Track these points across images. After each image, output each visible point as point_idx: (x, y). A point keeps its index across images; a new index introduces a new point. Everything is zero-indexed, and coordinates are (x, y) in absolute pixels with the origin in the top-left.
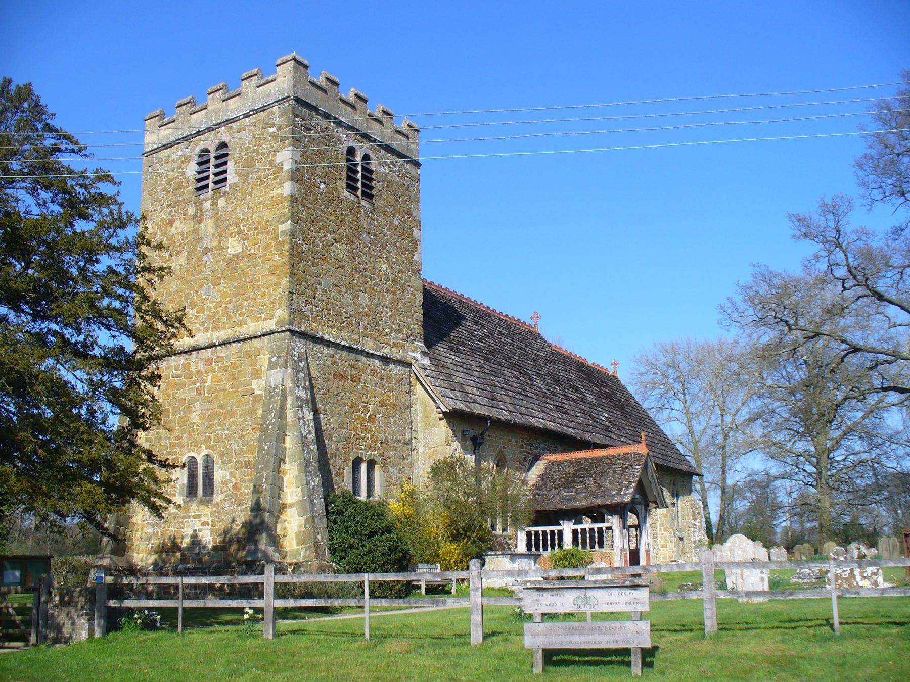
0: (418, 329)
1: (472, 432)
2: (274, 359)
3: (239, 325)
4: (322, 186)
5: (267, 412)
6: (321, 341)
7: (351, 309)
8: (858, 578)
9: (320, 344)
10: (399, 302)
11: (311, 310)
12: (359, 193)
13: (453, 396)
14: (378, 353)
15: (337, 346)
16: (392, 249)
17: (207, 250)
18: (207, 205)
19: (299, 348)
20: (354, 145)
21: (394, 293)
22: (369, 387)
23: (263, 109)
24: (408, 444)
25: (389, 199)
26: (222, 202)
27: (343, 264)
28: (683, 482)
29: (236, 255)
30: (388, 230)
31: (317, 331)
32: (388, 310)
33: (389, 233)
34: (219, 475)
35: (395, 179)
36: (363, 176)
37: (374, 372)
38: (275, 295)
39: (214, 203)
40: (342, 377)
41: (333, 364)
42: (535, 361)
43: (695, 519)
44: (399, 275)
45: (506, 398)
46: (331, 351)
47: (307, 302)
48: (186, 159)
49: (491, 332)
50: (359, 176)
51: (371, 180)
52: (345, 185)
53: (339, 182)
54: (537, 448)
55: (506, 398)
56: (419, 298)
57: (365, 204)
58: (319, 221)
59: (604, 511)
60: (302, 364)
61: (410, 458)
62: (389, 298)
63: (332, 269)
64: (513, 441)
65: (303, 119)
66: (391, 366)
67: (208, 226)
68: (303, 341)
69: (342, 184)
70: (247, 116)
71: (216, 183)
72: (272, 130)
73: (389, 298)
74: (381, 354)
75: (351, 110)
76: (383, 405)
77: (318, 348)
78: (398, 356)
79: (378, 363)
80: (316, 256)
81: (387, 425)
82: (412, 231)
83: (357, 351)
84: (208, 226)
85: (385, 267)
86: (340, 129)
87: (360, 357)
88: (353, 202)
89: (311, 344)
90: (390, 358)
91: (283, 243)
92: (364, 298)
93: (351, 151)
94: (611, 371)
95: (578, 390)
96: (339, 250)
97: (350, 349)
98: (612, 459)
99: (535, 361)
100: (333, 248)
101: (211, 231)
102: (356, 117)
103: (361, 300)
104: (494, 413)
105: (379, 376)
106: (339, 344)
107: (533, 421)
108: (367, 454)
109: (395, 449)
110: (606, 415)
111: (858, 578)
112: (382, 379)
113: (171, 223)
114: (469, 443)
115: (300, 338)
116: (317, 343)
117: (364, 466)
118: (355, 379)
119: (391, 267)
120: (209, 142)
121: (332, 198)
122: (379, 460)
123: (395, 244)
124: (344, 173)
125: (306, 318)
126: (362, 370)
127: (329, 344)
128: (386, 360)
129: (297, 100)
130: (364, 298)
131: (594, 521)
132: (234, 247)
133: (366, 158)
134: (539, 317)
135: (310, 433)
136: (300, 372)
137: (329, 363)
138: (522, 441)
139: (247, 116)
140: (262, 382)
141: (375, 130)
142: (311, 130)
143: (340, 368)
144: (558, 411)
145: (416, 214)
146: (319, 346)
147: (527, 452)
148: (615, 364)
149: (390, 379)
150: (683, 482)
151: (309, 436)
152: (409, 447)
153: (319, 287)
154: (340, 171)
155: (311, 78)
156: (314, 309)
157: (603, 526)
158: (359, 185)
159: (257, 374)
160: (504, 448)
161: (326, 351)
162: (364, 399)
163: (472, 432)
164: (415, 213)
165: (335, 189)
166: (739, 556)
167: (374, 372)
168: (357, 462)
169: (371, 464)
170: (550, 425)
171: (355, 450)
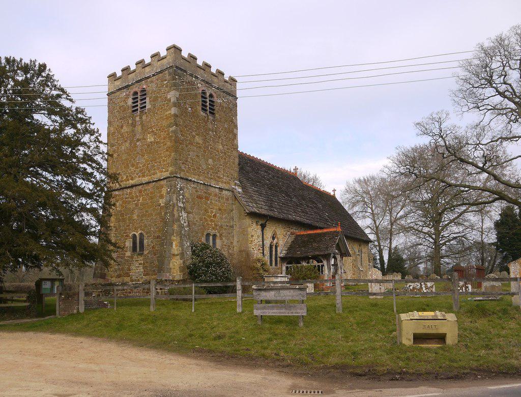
0: (236, 175)
1: (261, 222)
2: (169, 190)
3: (154, 174)
4: (190, 109)
5: (166, 213)
6: (190, 180)
7: (204, 167)
8: (424, 289)
12: (208, 112)
14: (217, 186)
17: (138, 140)
18: (138, 119)
21: (225, 159)
22: (213, 202)
23: (161, 72)
26: (144, 117)
29: (151, 142)
30: (222, 130)
34: (145, 241)
35: (225, 105)
36: (210, 104)
37: (216, 195)
38: (169, 161)
39: (141, 118)
40: (200, 197)
41: (197, 191)
42: (294, 190)
45: (278, 206)
47: (183, 163)
48: (127, 96)
49: (273, 177)
50: (208, 104)
51: (213, 106)
54: (292, 229)
55: (278, 206)
56: (237, 161)
57: (211, 117)
59: (320, 257)
60: (181, 192)
62: (222, 161)
67: (139, 128)
69: (199, 108)
70: (154, 75)
71: (141, 108)
72: (165, 82)
76: (220, 210)
78: (227, 188)
79: (217, 190)
81: (221, 218)
84: (139, 128)
88: (205, 117)
91: (172, 136)
93: (204, 93)
94: (332, 194)
95: (314, 203)
96: (198, 139)
98: (324, 234)
99: (294, 190)
101: (140, 131)
104: (271, 213)
108: (212, 232)
109: (225, 229)
111: (424, 289)
113: (122, 127)
114: (259, 227)
118: (207, 198)
119: (223, 147)
120: (136, 88)
121: (194, 114)
122: (218, 235)
125: (184, 171)
126: (210, 194)
129: (177, 67)
130: (210, 161)
131: (318, 262)
132: (150, 139)
133: (211, 96)
134: (297, 169)
135: (185, 223)
139: (154, 75)
140: (164, 200)
144: (303, 212)
148: (334, 191)
149: (223, 198)
157: (320, 264)
158: (208, 108)
159: (162, 197)
163: (261, 222)
165: (196, 111)
166: (374, 277)
167: (216, 195)
168: (208, 235)
169: (214, 236)
170: (298, 218)
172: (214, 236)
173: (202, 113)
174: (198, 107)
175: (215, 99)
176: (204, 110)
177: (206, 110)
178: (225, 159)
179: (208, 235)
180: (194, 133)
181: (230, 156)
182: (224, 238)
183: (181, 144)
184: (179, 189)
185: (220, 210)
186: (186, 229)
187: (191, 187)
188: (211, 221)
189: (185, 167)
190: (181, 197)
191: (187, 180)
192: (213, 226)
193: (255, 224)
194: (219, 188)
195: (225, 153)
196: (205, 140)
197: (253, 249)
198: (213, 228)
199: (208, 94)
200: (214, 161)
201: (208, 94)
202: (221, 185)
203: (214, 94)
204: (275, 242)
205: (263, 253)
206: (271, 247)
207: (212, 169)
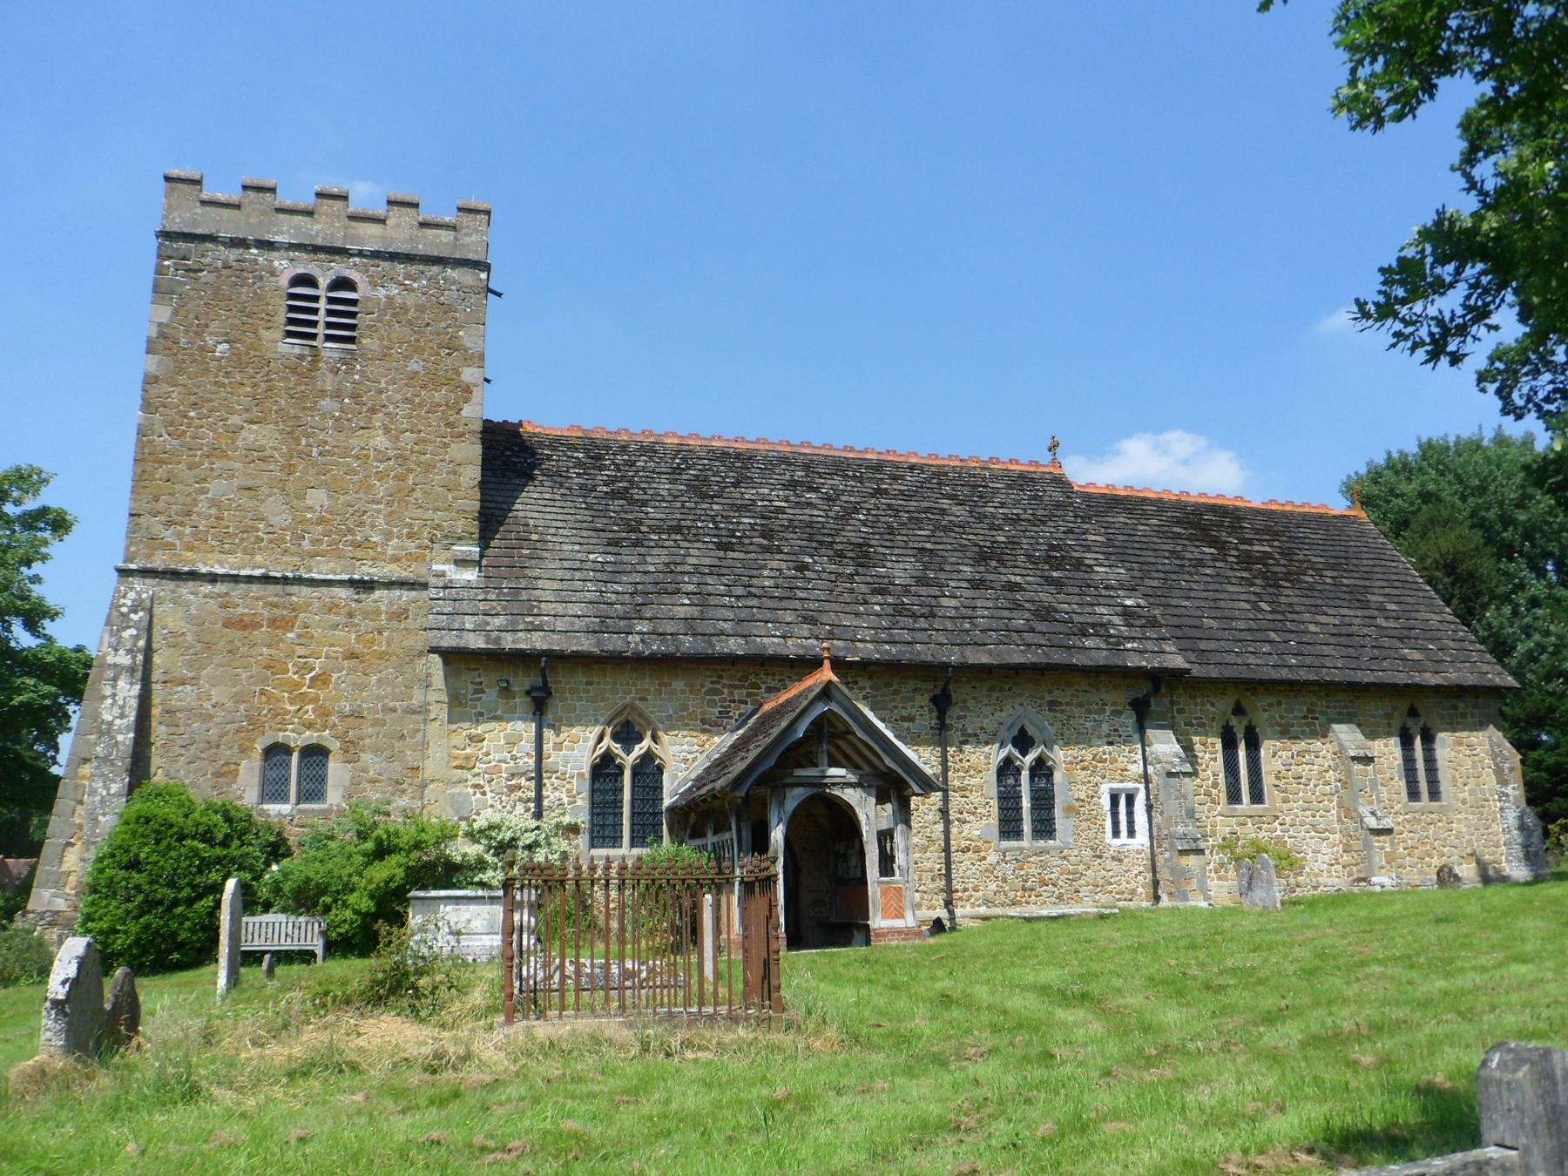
6: (193, 576)
9: (193, 580)
10: (413, 490)
11: (180, 535)
13: (468, 626)
14: (338, 577)
15: (235, 579)
16: (403, 410)
19: (137, 592)
20: (300, 271)
21: (400, 478)
24: (415, 712)
25: (394, 335)
27: (267, 453)
28: (1456, 708)
31: (187, 562)
32: (382, 506)
33: (391, 388)
35: (411, 300)
37: (332, 608)
40: (243, 625)
43: (1504, 783)
44: (416, 448)
46: (220, 588)
47: (169, 523)
52: (279, 335)
53: (265, 334)
58: (213, 400)
61: (419, 737)
62: (380, 488)
63: (238, 465)
64: (678, 685)
65: (184, 258)
66: (377, 594)
68: (148, 581)
73: (380, 488)
74: (345, 577)
75: (307, 219)
76: (352, 656)
77: (185, 590)
79: (343, 593)
80: (199, 453)
82: (459, 374)
83: (285, 580)
85: (380, 441)
86: (276, 254)
87: (295, 589)
88: (301, 357)
89: (171, 585)
90: (372, 582)
92: (317, 498)
97: (266, 579)
100: (244, 433)
102: (317, 227)
103: (309, 502)
105: (343, 611)
106: (238, 576)
107: (735, 646)
108: (297, 739)
109: (375, 723)
110: (1128, 602)
112: (350, 615)
115: (144, 577)
116: (187, 580)
117: (295, 757)
122: (334, 745)
123: (406, 400)
124: (282, 315)
125: (171, 546)
126: (295, 609)
127: (213, 578)
128: (365, 586)
130: (317, 498)
135: (122, 716)
136: (129, 627)
137: (212, 605)
138: (712, 683)
141: (370, 237)
142: (202, 271)
143: (240, 610)
145: (469, 345)
146: (191, 583)
147: (734, 701)
150: (1456, 708)
151: (118, 722)
152: (420, 718)
153: (203, 497)
154: (268, 318)
155: (205, 195)
156: (188, 530)
160: (643, 699)
161: (207, 588)
162: (300, 650)
163: (523, 681)
164: (467, 342)
167: (332, 608)
169: (315, 754)
171: (269, 733)
172: (315, 754)
173: (291, 348)
174: (265, 334)
175: (363, 291)
176: (299, 326)
177: (313, 336)
178: (400, 478)
179: (276, 752)
180: (235, 420)
181: (429, 467)
182: (367, 757)
183: (162, 462)
184: (124, 610)
185: (352, 656)
186: (120, 738)
187: (196, 594)
188: (303, 699)
189: (180, 535)
190: (127, 634)
191: (175, 575)
192: (311, 716)
193: (491, 695)
194: (352, 583)
195: (401, 459)
196: (292, 433)
197: (476, 786)
198: (310, 726)
199: (323, 282)
200: (333, 491)
201: (323, 282)
202: (364, 571)
203: (354, 275)
204: (629, 759)
205: (539, 799)
206: (605, 769)
207: (321, 521)
